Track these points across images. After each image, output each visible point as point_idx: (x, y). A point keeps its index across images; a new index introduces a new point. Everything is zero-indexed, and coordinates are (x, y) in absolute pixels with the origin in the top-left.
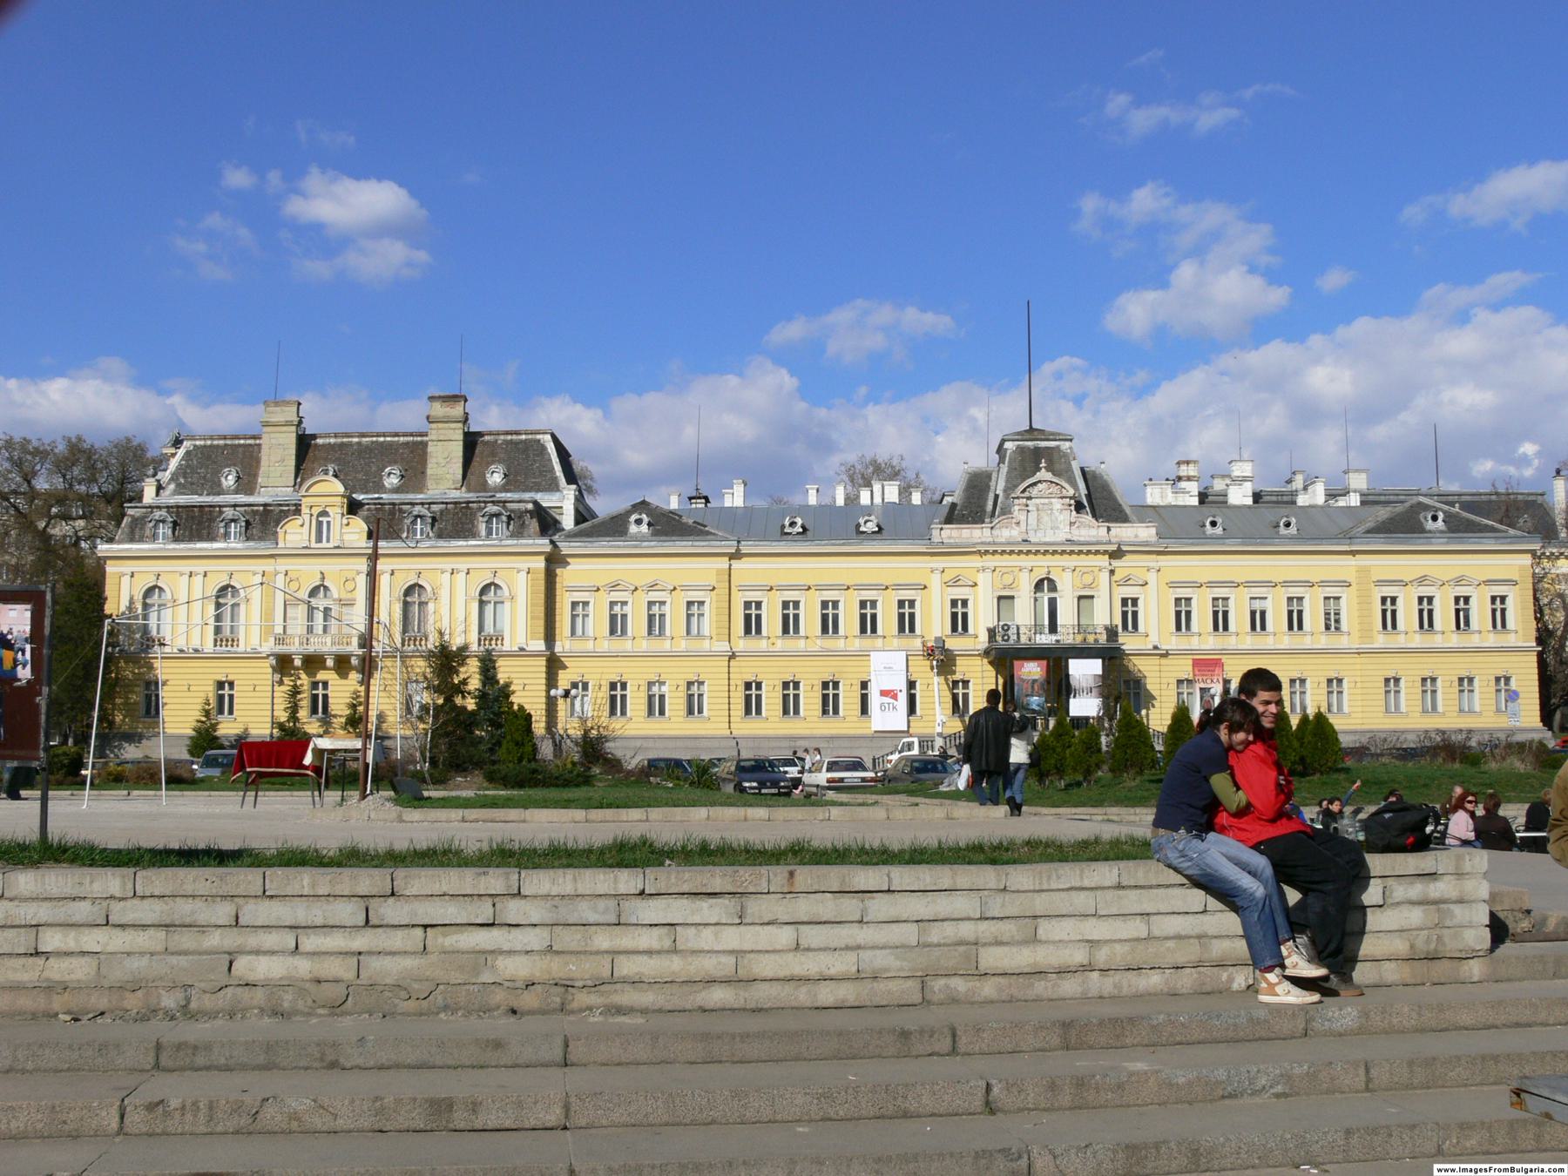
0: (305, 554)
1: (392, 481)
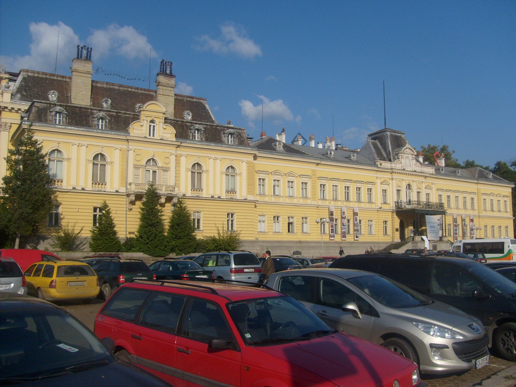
0: (144, 141)
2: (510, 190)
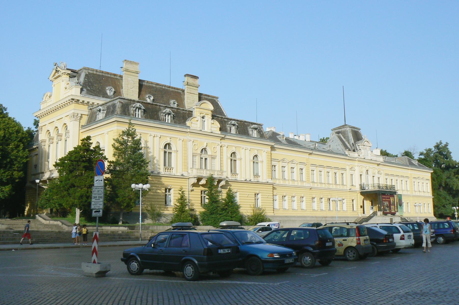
2: (429, 175)
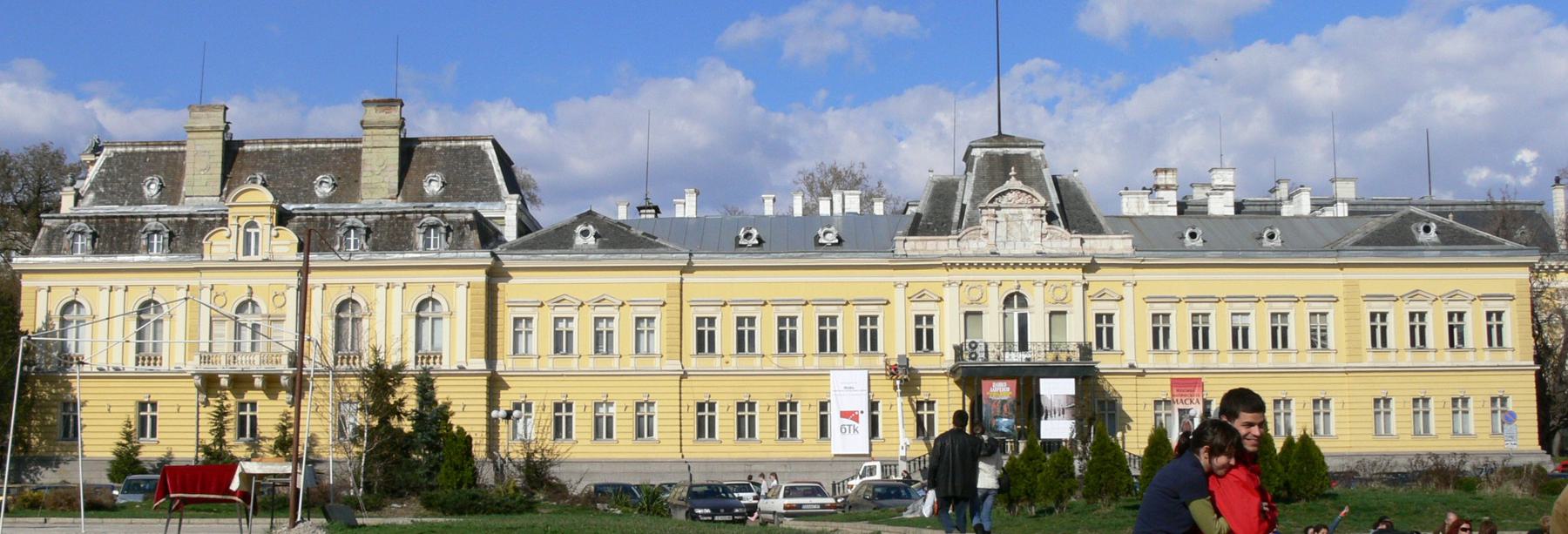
0: (232, 267)
1: (324, 190)
